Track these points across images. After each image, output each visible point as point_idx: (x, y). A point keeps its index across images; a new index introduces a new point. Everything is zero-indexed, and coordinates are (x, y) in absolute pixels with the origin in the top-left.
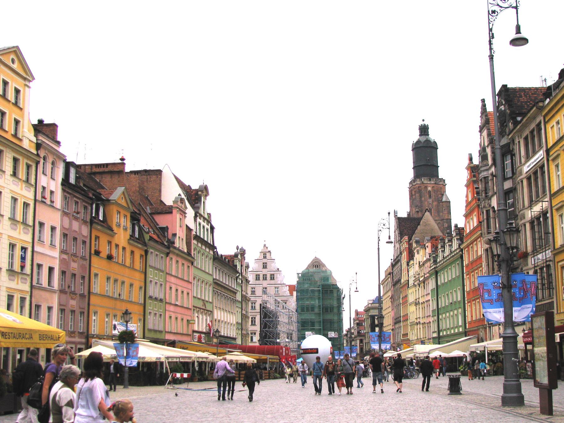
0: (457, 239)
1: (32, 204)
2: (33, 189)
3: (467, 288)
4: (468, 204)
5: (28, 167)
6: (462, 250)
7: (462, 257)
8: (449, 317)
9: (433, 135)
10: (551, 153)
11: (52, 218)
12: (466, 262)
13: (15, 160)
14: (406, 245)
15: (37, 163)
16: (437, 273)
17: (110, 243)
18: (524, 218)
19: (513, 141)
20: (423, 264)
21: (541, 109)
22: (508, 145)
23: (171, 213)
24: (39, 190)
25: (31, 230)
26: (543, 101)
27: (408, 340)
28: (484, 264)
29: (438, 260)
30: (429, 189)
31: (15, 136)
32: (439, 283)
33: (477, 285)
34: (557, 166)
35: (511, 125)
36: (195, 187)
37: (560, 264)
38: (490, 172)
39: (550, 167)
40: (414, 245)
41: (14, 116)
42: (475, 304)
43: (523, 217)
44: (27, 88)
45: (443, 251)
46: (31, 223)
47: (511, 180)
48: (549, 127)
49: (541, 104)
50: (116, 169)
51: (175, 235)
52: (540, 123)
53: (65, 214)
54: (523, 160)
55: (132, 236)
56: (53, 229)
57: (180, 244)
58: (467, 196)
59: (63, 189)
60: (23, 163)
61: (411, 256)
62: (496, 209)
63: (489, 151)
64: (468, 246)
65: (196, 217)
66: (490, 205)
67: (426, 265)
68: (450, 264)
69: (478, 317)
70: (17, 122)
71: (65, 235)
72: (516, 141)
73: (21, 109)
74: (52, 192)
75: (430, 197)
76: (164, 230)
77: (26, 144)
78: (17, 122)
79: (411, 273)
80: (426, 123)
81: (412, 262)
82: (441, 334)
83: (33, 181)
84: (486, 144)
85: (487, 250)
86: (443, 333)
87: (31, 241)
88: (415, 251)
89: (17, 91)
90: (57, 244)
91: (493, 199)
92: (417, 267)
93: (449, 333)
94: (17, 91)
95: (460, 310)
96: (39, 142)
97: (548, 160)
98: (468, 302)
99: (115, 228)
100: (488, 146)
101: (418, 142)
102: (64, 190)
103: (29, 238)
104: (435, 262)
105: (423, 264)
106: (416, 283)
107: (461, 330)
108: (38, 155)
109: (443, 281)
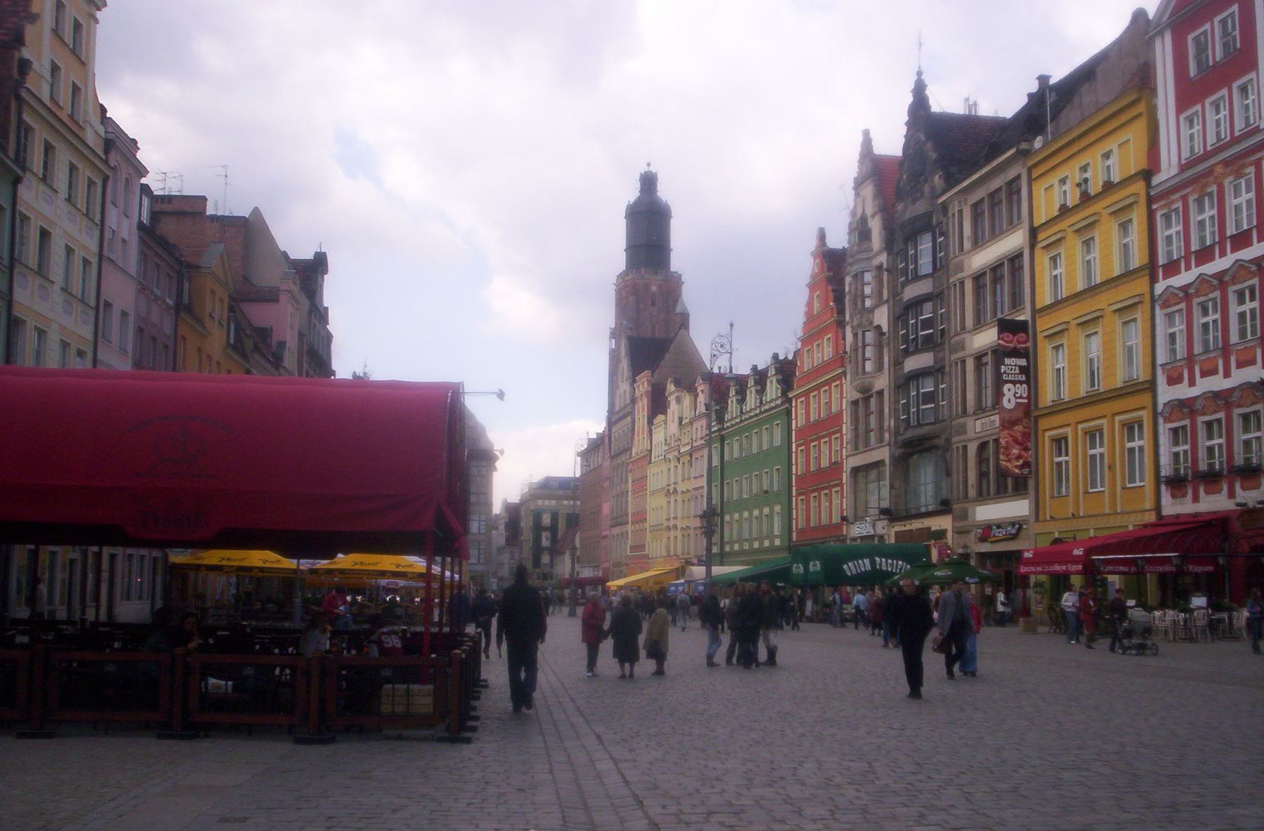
0: (778, 381)
1: (94, 260)
2: (97, 233)
3: (798, 469)
4: (810, 318)
5: (91, 183)
6: (790, 401)
7: (789, 412)
8: (739, 522)
9: (664, 192)
10: (1041, 237)
11: (122, 293)
12: (798, 421)
13: (73, 168)
14: (643, 386)
15: (105, 180)
16: (722, 439)
17: (200, 350)
18: (963, 348)
19: (945, 207)
20: (691, 424)
21: (1026, 154)
22: (928, 215)
23: (277, 301)
24: (108, 235)
25: (92, 314)
26: (1031, 141)
27: (647, 556)
28: (846, 428)
29: (727, 417)
30: (654, 288)
31: (71, 116)
32: (726, 458)
33: (825, 463)
34: (1054, 259)
35: (937, 180)
36: (309, 255)
37: (1048, 434)
38: (876, 262)
39: (1037, 261)
40: (671, 387)
41: (72, 78)
42: (818, 499)
43: (962, 346)
44: (92, 23)
45: (742, 401)
46: (93, 303)
47: (930, 280)
48: (1039, 189)
49: (1024, 146)
50: (188, 209)
51: (282, 345)
52: (1018, 177)
53: (143, 289)
54: (967, 245)
55: (228, 344)
56: (124, 314)
57: (290, 360)
58: (810, 304)
59: (140, 238)
60: (85, 172)
61: (658, 405)
62: (885, 329)
63: (875, 225)
64: (806, 394)
65: (311, 312)
66: (871, 323)
67: (697, 425)
68: (759, 424)
69: (824, 521)
70: (76, 89)
71: (140, 330)
72: (954, 208)
73: (83, 64)
74: (124, 241)
75: (653, 304)
76: (264, 333)
77: (90, 138)
78: (76, 89)
79: (659, 436)
80: (653, 169)
81: (660, 418)
82: (727, 548)
83: (97, 218)
84: (869, 211)
85: (855, 403)
86: (732, 547)
87: (90, 336)
88: (672, 399)
89: (77, 26)
90: (130, 347)
91: (877, 312)
92: (673, 428)
93: (746, 547)
94: (77, 26)
95: (777, 508)
96: (110, 136)
97: (1032, 247)
98: (798, 494)
99: (207, 321)
100: (873, 216)
101: (638, 203)
102: (142, 242)
103: (87, 332)
104: (720, 419)
105: (691, 424)
106: (670, 456)
107: (777, 542)
108: (106, 162)
109: (736, 455)
